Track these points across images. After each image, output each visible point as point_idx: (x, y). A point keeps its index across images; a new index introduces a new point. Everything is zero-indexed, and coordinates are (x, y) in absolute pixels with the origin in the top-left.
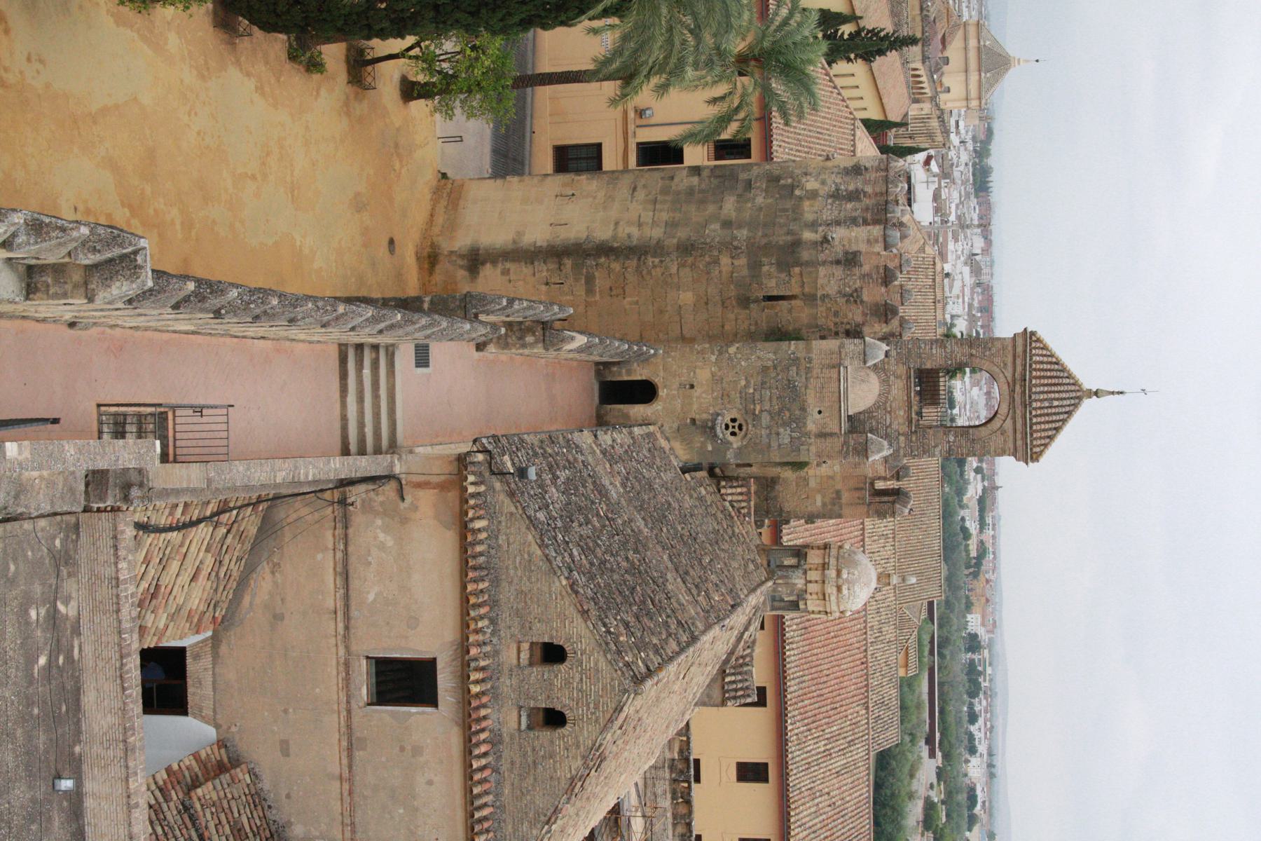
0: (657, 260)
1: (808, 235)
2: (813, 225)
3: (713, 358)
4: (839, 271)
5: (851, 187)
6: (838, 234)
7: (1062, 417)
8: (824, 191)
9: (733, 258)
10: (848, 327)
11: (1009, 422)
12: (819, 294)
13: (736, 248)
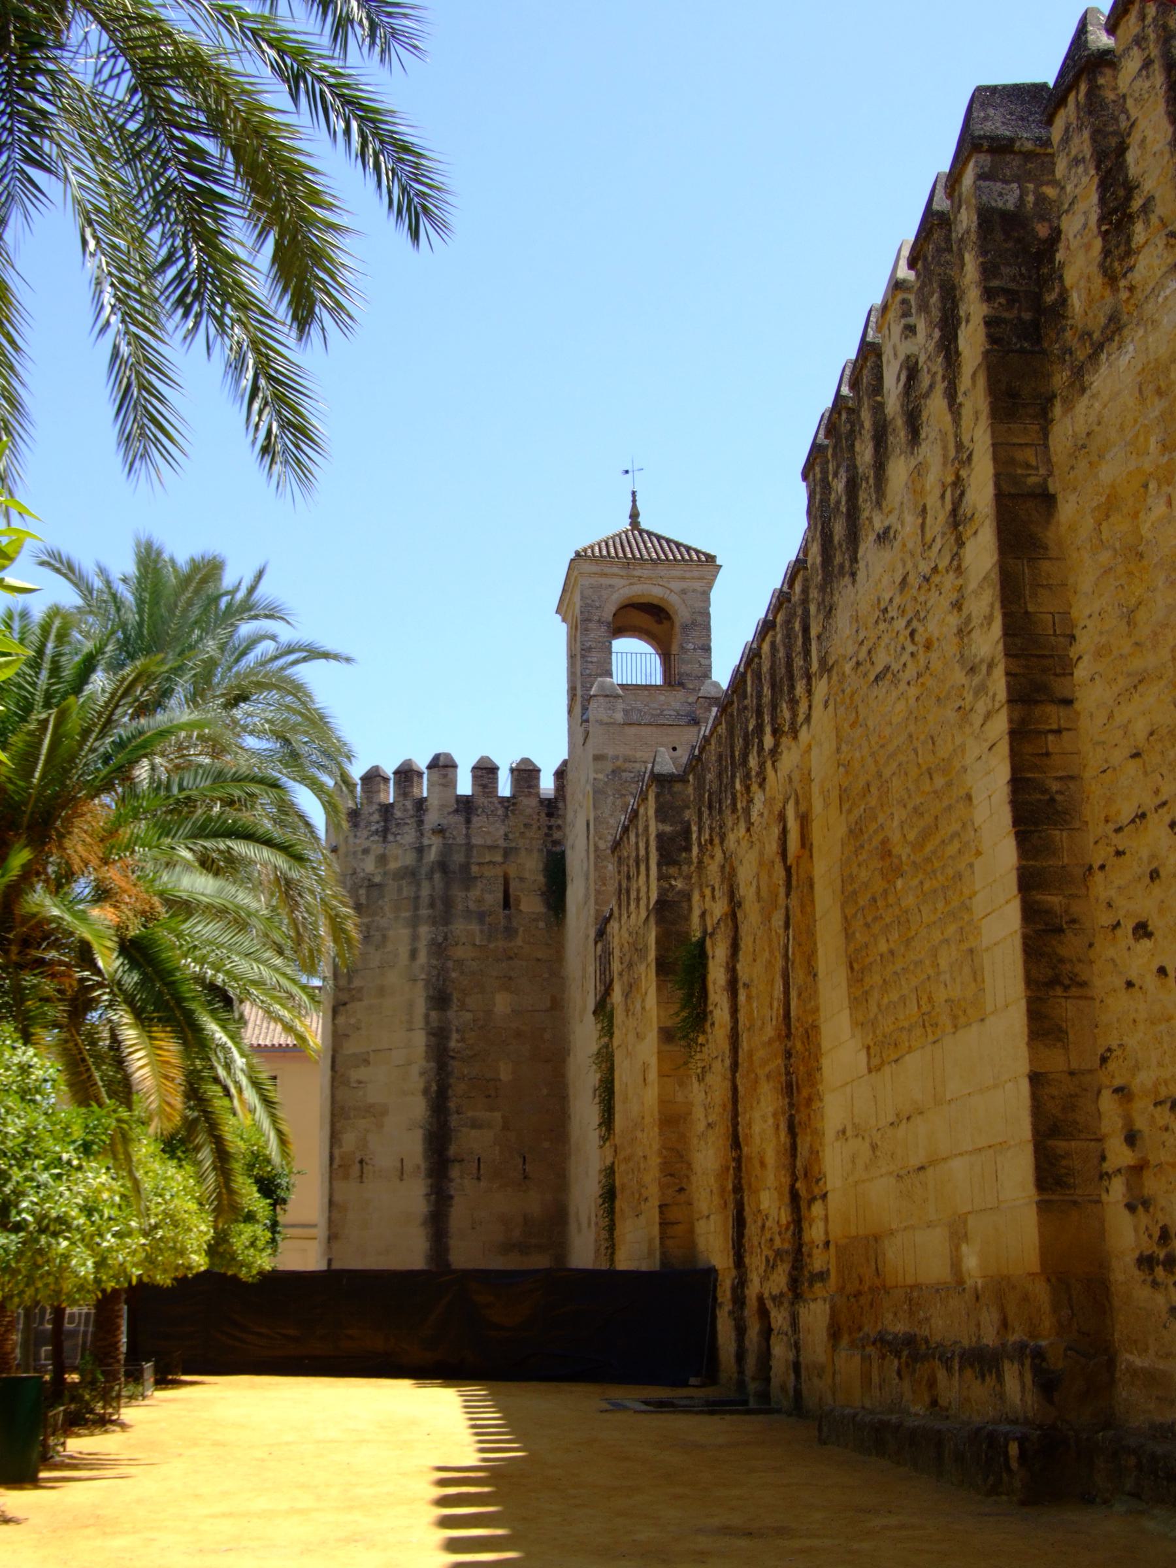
0: (455, 1036)
1: (432, 855)
2: (420, 850)
5: (376, 817)
6: (432, 818)
7: (665, 545)
8: (377, 849)
10: (543, 815)
12: (501, 843)
13: (446, 938)
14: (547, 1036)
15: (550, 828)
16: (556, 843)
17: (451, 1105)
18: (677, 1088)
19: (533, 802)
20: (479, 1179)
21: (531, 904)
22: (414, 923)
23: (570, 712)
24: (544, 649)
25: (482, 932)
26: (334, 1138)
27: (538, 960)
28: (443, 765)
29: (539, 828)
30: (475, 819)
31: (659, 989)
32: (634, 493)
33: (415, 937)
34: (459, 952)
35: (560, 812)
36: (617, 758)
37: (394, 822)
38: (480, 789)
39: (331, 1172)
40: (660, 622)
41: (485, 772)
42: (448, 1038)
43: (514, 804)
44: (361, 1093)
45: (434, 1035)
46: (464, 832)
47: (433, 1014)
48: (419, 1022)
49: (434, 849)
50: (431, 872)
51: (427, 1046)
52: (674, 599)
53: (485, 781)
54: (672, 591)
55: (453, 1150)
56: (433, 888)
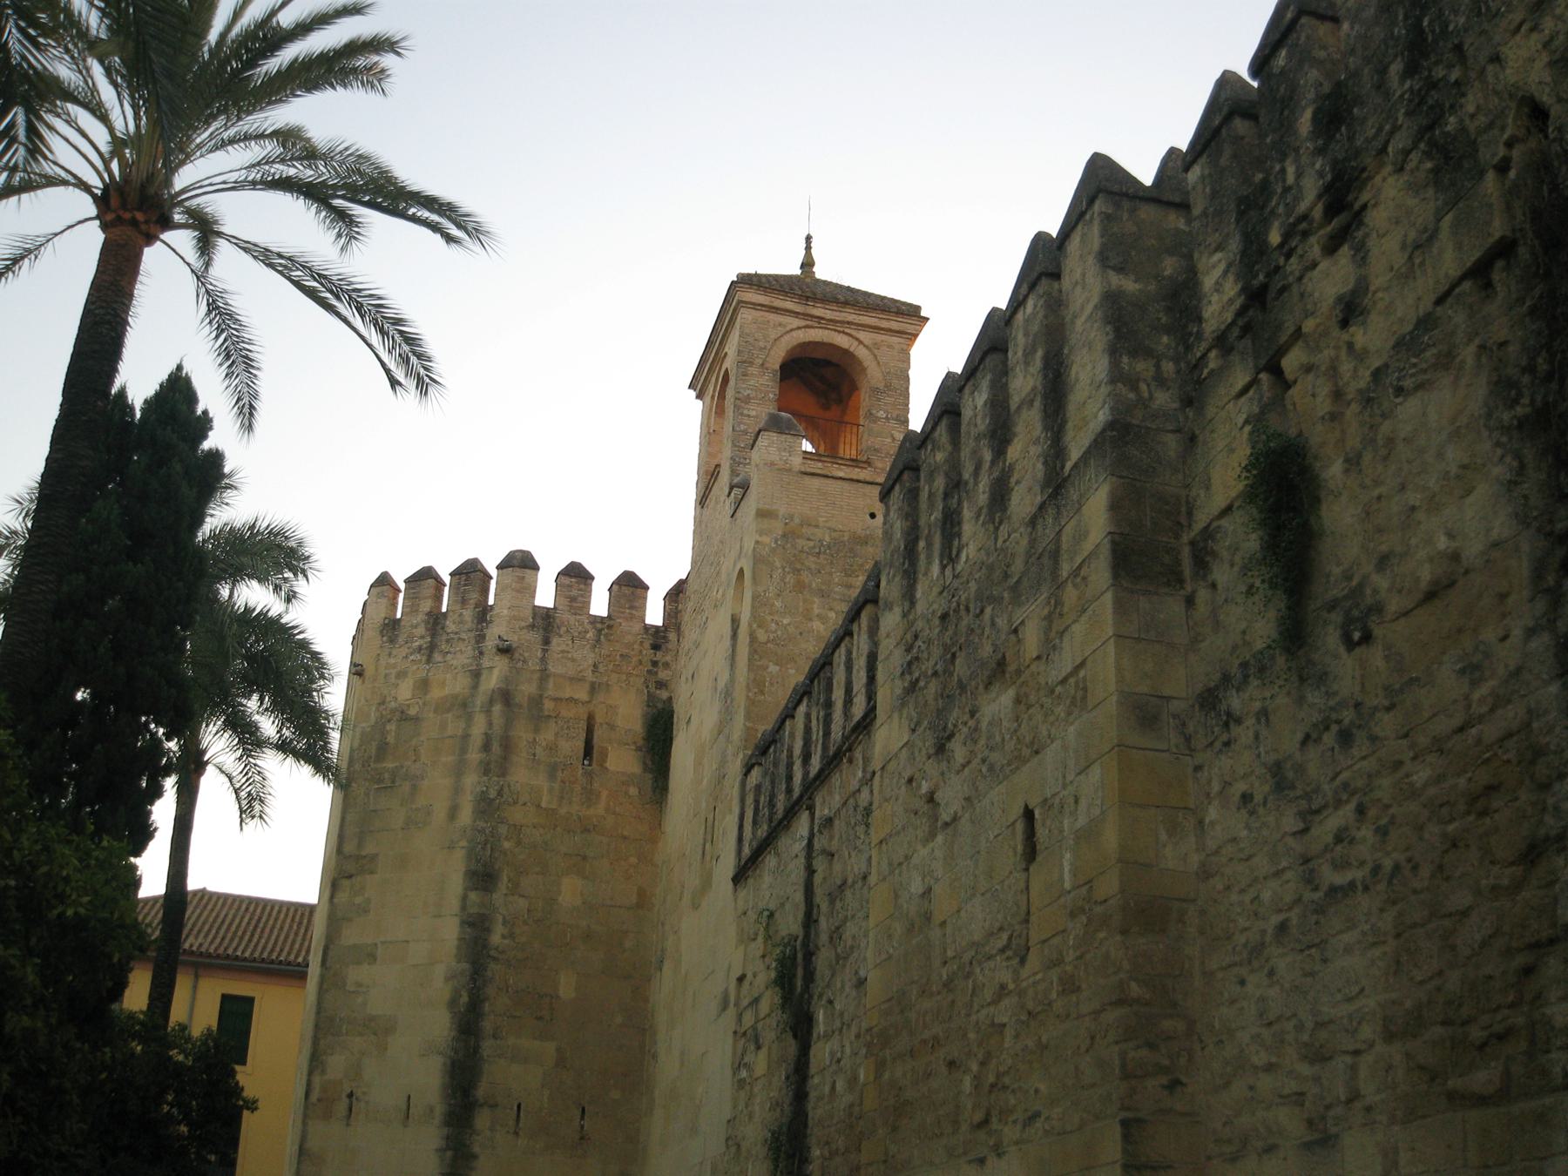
1: (491, 681)
2: (476, 675)
3: (773, 668)
4: (557, 644)
5: (421, 630)
9: (515, 803)
10: (647, 644)
11: (862, 335)
12: (589, 674)
13: (500, 793)
14: (628, 944)
15: (655, 664)
16: (661, 685)
17: (487, 1025)
18: (1163, 837)
19: (637, 627)
20: (516, 1133)
21: (623, 761)
22: (458, 771)
23: (702, 500)
24: (669, 435)
25: (551, 790)
26: (316, 1061)
27: (625, 838)
28: (521, 564)
29: (640, 662)
30: (555, 641)
31: (1120, 608)
32: (808, 239)
33: (457, 790)
34: (517, 815)
35: (670, 646)
36: (792, 517)
37: (444, 637)
38: (566, 602)
39: (306, 1107)
40: (826, 407)
41: (576, 577)
42: (488, 930)
43: (610, 627)
44: (360, 1000)
45: (471, 925)
46: (539, 654)
47: (473, 896)
48: (454, 903)
49: (496, 672)
50: (491, 702)
51: (460, 939)
52: (861, 353)
53: (574, 593)
54: (861, 342)
55: (481, 1092)
56: (490, 724)
